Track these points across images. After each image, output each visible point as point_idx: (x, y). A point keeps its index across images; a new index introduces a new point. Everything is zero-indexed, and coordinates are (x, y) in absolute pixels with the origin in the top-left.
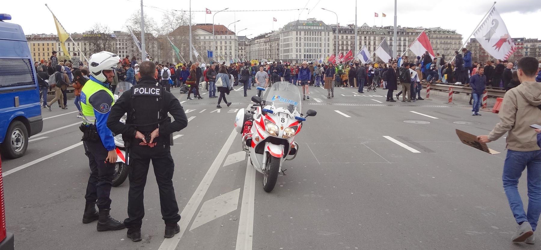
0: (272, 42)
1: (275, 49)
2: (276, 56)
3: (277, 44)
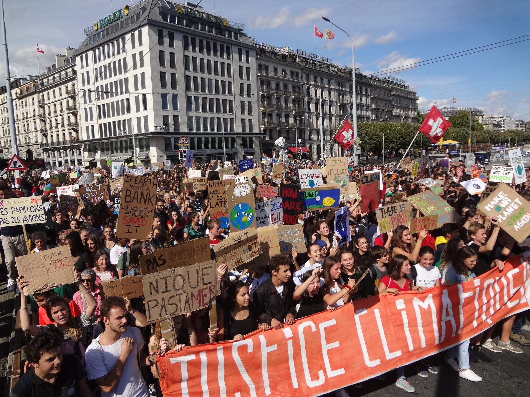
0: (45, 93)
1: (62, 110)
2: (67, 133)
3: (67, 92)
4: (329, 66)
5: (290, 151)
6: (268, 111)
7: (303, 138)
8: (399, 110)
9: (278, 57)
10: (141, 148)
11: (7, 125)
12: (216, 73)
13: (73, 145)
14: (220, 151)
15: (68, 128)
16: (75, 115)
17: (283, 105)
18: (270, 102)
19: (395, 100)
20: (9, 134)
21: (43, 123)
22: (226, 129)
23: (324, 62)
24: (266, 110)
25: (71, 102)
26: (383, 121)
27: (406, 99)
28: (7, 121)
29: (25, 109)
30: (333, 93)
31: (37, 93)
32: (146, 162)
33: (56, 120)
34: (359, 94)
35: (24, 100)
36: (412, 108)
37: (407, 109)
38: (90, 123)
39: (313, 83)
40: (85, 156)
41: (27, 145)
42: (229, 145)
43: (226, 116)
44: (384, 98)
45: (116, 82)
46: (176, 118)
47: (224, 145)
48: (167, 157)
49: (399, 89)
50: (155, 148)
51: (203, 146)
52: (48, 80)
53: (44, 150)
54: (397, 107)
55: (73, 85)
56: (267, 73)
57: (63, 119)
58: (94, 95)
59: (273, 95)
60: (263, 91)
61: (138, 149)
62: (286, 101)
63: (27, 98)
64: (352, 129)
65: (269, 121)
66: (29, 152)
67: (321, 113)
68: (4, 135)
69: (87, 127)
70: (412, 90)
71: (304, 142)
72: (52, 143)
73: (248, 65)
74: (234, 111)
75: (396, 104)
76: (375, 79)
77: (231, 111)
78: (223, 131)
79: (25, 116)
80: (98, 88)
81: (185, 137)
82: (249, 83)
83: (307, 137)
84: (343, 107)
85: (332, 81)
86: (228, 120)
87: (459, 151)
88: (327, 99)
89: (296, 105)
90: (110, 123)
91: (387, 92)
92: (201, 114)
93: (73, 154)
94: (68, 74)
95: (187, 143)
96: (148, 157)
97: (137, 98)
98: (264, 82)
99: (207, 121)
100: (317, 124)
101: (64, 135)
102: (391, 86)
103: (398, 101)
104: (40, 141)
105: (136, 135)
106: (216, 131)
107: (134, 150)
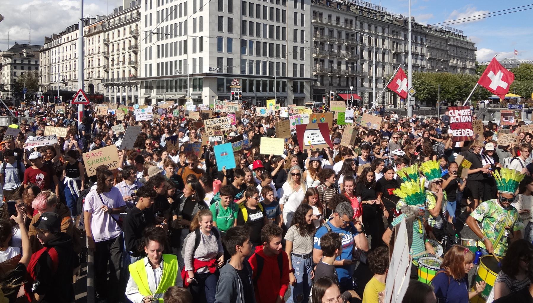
0: (111, 32)
1: (124, 49)
3: (131, 33)
4: (383, 15)
5: (340, 97)
6: (320, 57)
7: (355, 85)
8: (455, 60)
9: (332, 5)
10: (195, 87)
11: (74, 60)
12: (271, 19)
13: (132, 81)
14: (271, 94)
15: (128, 65)
16: (136, 53)
17: (336, 51)
18: (322, 48)
19: (452, 50)
20: (75, 68)
21: (106, 60)
22: (278, 73)
23: (378, 10)
24: (319, 57)
25: (133, 41)
26: (439, 71)
27: (463, 50)
28: (74, 57)
29: (91, 46)
30: (387, 42)
31: (104, 31)
32: (198, 101)
33: (118, 58)
34: (415, 43)
35: (91, 38)
36: (470, 59)
37: (464, 60)
38: (148, 62)
39: (367, 31)
40: (142, 93)
41: (90, 79)
42: (280, 89)
43: (278, 60)
44: (440, 48)
45: (176, 24)
46: (230, 60)
47: (274, 89)
48: (219, 97)
49: (456, 40)
50: (208, 88)
51: (254, 88)
52: (114, 20)
53: (105, 85)
54: (454, 57)
55: (137, 26)
56: (321, 20)
57: (124, 57)
58: (154, 37)
59: (325, 41)
60: (316, 37)
61: (191, 89)
62: (339, 48)
63: (94, 37)
64: (407, 78)
65: (321, 67)
66: (91, 87)
67: (374, 61)
68: (70, 69)
69: (146, 65)
70: (470, 41)
71: (355, 89)
72: (113, 79)
73: (303, 12)
74: (287, 56)
75: (452, 55)
76: (431, 29)
77: (284, 56)
78: (274, 75)
79: (91, 53)
80: (159, 29)
81: (238, 80)
82: (303, 29)
83: (359, 85)
84: (397, 55)
85: (386, 30)
86: (281, 64)
87: (521, 106)
88: (381, 47)
89: (349, 53)
90: (167, 63)
91: (443, 42)
92: (254, 58)
93: (131, 91)
94: (133, 16)
95: (239, 85)
96: (200, 97)
97: (194, 40)
98: (318, 28)
99: (259, 65)
100: (369, 71)
101: (124, 71)
102: (448, 36)
103: (455, 51)
104: (101, 76)
105: (191, 75)
106: (268, 75)
107: (188, 90)
